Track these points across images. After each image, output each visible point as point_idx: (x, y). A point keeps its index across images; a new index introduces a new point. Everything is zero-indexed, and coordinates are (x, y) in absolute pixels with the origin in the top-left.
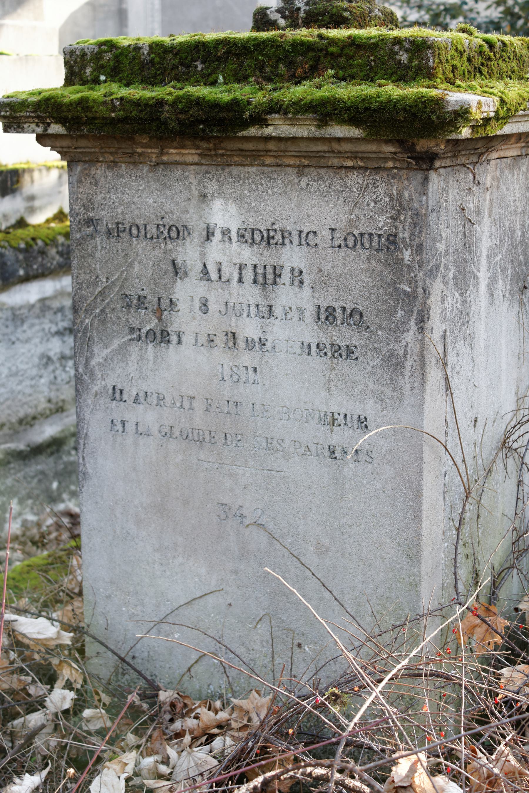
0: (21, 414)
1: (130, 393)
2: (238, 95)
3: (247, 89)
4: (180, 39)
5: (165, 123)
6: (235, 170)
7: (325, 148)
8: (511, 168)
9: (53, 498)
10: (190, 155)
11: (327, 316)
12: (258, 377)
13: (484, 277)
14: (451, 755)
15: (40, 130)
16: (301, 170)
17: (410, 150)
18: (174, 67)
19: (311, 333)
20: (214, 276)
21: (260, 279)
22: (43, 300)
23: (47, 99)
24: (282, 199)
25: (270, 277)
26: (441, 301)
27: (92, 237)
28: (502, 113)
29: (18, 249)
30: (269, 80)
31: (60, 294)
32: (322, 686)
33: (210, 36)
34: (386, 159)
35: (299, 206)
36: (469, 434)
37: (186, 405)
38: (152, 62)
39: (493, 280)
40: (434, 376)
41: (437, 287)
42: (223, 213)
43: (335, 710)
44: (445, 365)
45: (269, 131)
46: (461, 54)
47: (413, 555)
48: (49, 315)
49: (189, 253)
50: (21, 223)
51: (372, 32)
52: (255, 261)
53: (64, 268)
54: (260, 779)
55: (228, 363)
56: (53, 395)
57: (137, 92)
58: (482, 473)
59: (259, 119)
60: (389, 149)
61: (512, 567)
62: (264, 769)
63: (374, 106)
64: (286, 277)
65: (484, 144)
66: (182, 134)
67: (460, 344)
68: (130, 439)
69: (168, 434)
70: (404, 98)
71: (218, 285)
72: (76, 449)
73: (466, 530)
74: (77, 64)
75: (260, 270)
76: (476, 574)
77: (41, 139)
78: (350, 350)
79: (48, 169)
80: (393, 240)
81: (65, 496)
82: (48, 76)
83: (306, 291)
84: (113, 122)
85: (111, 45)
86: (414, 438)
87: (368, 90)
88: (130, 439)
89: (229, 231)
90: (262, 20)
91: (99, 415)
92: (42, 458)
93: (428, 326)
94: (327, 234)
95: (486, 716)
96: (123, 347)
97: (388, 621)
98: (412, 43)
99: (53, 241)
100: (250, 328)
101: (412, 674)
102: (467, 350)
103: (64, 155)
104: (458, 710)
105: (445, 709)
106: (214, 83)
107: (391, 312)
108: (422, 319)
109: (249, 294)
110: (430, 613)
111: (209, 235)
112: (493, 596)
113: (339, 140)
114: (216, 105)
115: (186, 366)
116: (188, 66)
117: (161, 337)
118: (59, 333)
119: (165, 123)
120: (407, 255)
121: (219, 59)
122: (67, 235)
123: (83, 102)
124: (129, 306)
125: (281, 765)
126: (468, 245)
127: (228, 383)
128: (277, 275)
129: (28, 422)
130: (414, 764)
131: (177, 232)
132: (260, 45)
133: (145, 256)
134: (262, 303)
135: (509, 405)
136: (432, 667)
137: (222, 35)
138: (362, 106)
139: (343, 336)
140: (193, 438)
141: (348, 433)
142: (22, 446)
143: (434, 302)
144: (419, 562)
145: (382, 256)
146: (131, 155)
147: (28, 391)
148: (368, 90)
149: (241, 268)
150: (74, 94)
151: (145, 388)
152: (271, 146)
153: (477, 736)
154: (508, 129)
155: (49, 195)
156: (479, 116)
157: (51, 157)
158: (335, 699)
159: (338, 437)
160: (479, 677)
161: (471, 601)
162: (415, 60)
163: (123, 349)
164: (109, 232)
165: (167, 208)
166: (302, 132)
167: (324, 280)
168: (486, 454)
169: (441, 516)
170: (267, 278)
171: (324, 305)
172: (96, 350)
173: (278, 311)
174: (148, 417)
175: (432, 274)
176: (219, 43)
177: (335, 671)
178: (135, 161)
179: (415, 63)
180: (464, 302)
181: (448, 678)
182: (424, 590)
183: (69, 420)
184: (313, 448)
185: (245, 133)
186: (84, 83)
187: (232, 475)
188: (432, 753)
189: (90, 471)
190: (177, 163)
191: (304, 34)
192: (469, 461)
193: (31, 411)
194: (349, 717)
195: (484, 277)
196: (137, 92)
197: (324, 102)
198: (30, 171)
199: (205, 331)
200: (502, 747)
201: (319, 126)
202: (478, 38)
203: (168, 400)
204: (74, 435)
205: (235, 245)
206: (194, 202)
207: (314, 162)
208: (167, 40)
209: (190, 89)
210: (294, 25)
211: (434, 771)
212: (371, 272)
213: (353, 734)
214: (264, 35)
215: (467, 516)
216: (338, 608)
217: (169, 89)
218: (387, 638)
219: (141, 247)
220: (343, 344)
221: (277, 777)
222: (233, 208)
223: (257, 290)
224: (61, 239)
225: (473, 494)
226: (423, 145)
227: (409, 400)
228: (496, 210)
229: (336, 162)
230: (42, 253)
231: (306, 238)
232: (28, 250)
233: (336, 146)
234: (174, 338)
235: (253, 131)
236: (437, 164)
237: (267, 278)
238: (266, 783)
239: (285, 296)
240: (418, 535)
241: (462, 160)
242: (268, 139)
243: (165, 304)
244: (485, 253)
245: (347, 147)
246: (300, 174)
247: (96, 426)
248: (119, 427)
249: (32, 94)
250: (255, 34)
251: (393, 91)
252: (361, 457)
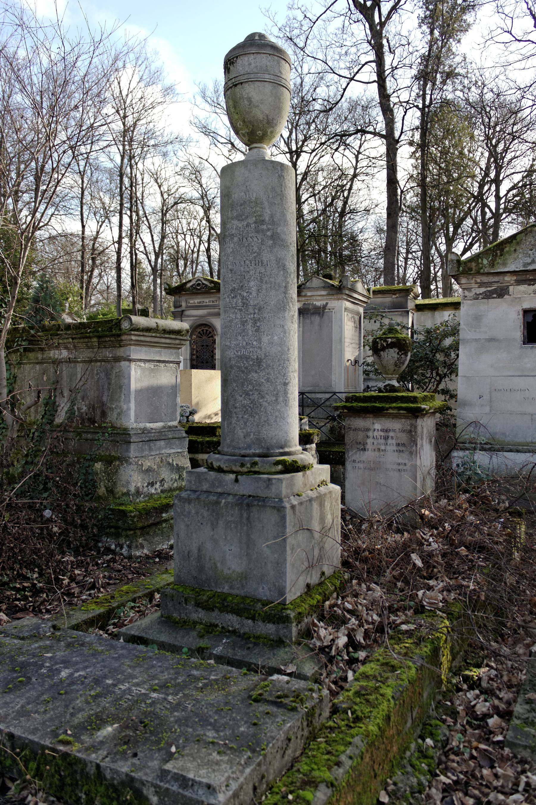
11: (398, 445)
19: (395, 448)
42: (377, 426)
49: (370, 434)
86: (415, 467)
100: (383, 447)
109: (383, 441)
115: (369, 455)
117: (364, 450)
131: (368, 430)
133: (361, 435)
139: (401, 448)
140: (371, 469)
159: (401, 467)
167: (397, 438)
174: (361, 465)
231: (394, 431)
237: (386, 438)
239: (390, 441)
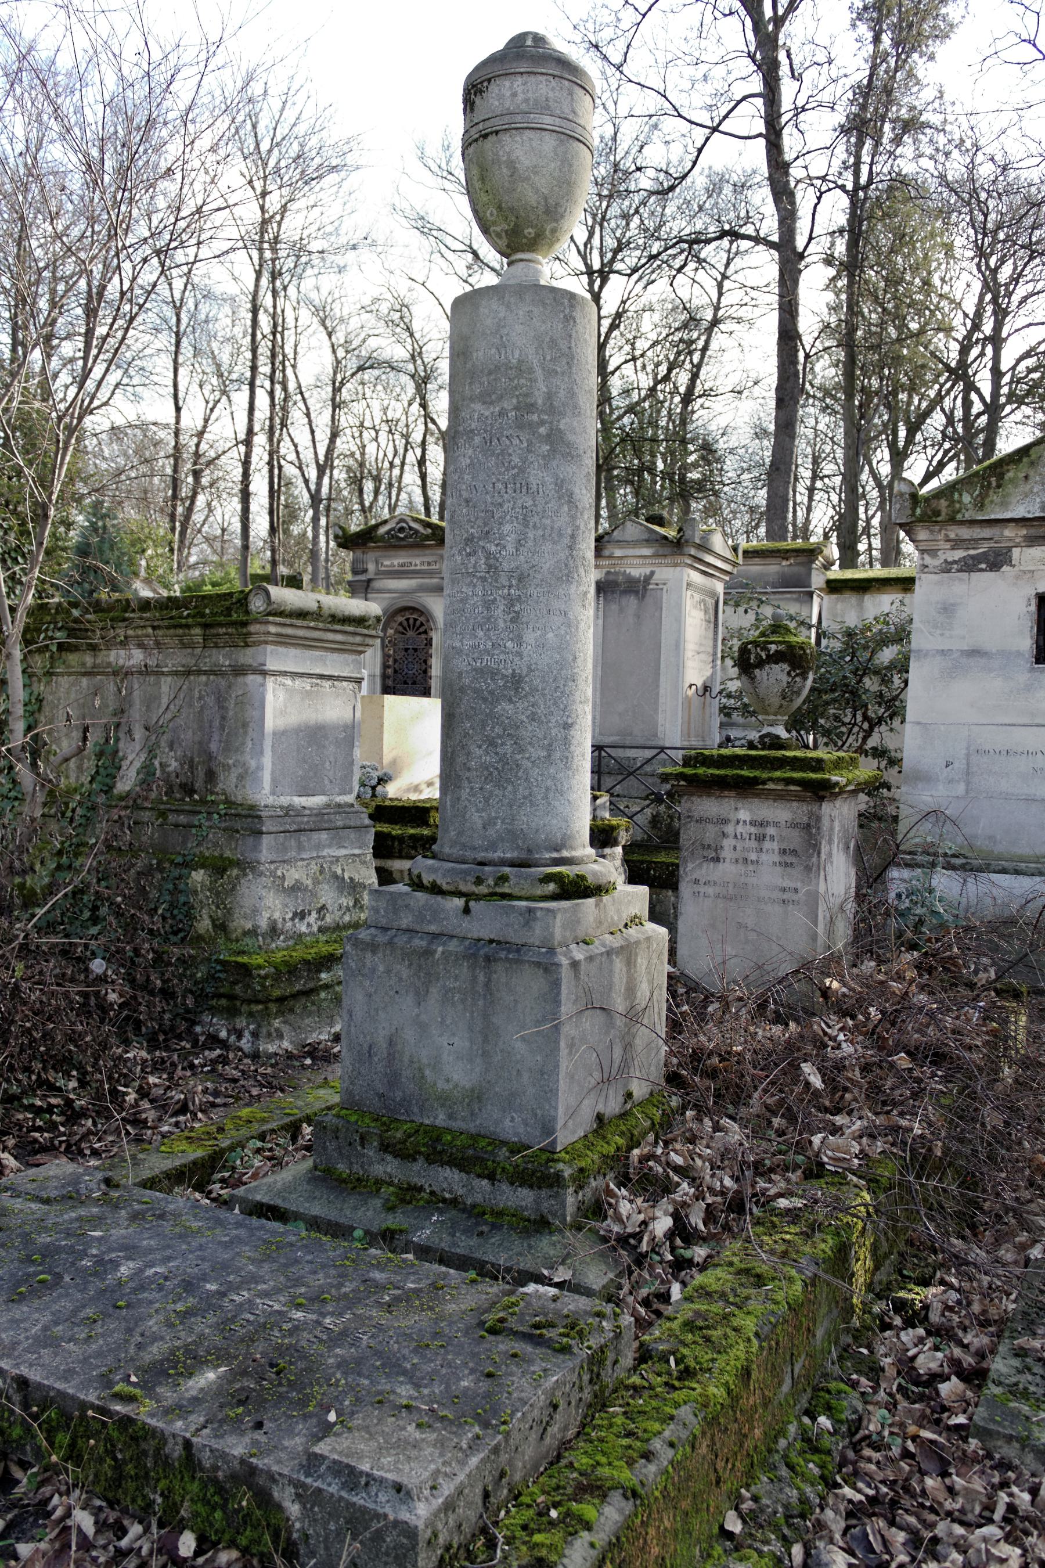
10: (733, 794)
11: (784, 852)
19: (777, 858)
26: (824, 849)
42: (744, 815)
49: (729, 829)
100: (753, 856)
109: (754, 844)
115: (727, 870)
117: (717, 860)
131: (725, 821)
139: (789, 859)
140: (728, 898)
167: (782, 839)
174: (710, 890)
178: (709, 795)
219: (710, 826)
231: (776, 824)
237: (761, 838)
239: (767, 845)
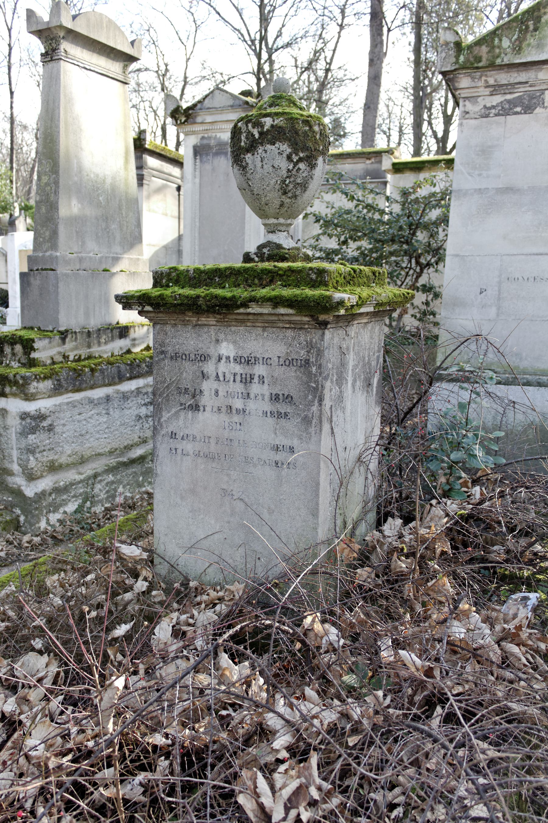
0: (126, 444)
1: (180, 434)
2: (235, 293)
3: (240, 290)
4: (208, 267)
5: (200, 306)
6: (233, 329)
7: (276, 318)
8: (364, 328)
9: (140, 485)
10: (212, 320)
11: (275, 398)
12: (242, 427)
13: (350, 379)
14: (332, 613)
15: (140, 309)
16: (264, 328)
17: (316, 320)
18: (205, 280)
19: (268, 407)
20: (221, 378)
21: (244, 380)
22: (138, 389)
23: (144, 294)
24: (255, 343)
25: (249, 379)
26: (330, 391)
27: (163, 359)
28: (360, 303)
29: (128, 364)
30: (250, 286)
31: (147, 385)
32: (270, 579)
33: (223, 265)
34: (305, 324)
35: (263, 346)
36: (342, 454)
37: (207, 441)
38: (195, 277)
39: (355, 381)
40: (326, 427)
41: (328, 384)
42: (227, 349)
43: (276, 591)
44: (331, 422)
45: (250, 310)
46: (341, 275)
47: (315, 513)
48: (141, 396)
49: (210, 368)
50: (129, 352)
51: (298, 265)
52: (242, 372)
53: (149, 373)
54: (239, 626)
55: (227, 420)
56: (141, 435)
57: (188, 291)
58: (349, 474)
59: (245, 305)
60: (306, 319)
61: (362, 519)
62: (241, 622)
63: (299, 299)
64: (256, 380)
65: (351, 317)
66: (208, 311)
67: (339, 412)
68: (179, 458)
69: (198, 455)
70: (314, 295)
71: (223, 383)
72: (152, 461)
73: (340, 501)
74: (159, 279)
75: (244, 376)
76: (345, 523)
77: (140, 313)
78: (286, 414)
79: (143, 326)
80: (307, 362)
81: (146, 484)
82: (145, 284)
83: (266, 386)
84: (175, 306)
85: (175, 269)
86: (316, 456)
87: (297, 291)
88: (179, 458)
89: (229, 357)
90: (247, 258)
91: (164, 446)
92: (135, 465)
93: (324, 403)
94: (276, 359)
95: (349, 593)
96: (177, 413)
97: (302, 546)
98: (318, 270)
99: (144, 360)
100: (238, 404)
101: (314, 572)
102: (342, 415)
103: (151, 320)
104: (336, 590)
105: (329, 590)
106: (224, 288)
107: (306, 397)
108: (321, 400)
109: (239, 387)
110: (323, 542)
111: (220, 359)
112: (353, 534)
113: (282, 315)
114: (225, 298)
115: (207, 422)
116: (212, 279)
117: (196, 408)
118: (145, 405)
119: (200, 306)
120: (314, 369)
121: (226, 276)
122: (151, 358)
123: (161, 296)
124: (180, 393)
125: (250, 619)
126: (343, 364)
127: (227, 430)
128: (252, 378)
129: (128, 448)
130: (314, 618)
131: (204, 358)
132: (246, 270)
133: (189, 370)
134: (243, 391)
135: (362, 441)
136: (323, 569)
137: (228, 265)
138: (294, 299)
139: (283, 408)
140: (209, 457)
141: (285, 454)
142: (125, 460)
143: (326, 392)
144: (318, 517)
145: (302, 370)
146: (183, 321)
147: (129, 432)
148: (297, 291)
149: (235, 375)
150: (156, 292)
151: (187, 432)
152: (250, 317)
153: (345, 604)
154: (362, 310)
155: (142, 338)
156: (349, 304)
157: (144, 320)
158: (276, 585)
159: (279, 457)
160: (345, 574)
161: (343, 536)
162: (320, 278)
163: (177, 413)
164: (172, 358)
165: (200, 346)
166: (265, 311)
167: (274, 381)
168: (350, 464)
169: (329, 494)
170: (247, 380)
171: (274, 393)
172: (164, 414)
173: (252, 396)
174: (189, 447)
175: (326, 378)
176: (226, 269)
177: (277, 571)
178: (185, 323)
179: (319, 279)
180: (341, 392)
181: (331, 575)
182: (320, 531)
183: (149, 447)
184: (267, 462)
185: (238, 311)
186: (162, 287)
187: (228, 475)
188: (323, 612)
189: (159, 473)
190: (205, 325)
191: (267, 265)
192: (342, 468)
193: (130, 443)
194: (283, 595)
195: (350, 379)
196: (188, 291)
197: (276, 297)
198: (134, 327)
199: (217, 404)
200: (357, 609)
201: (273, 308)
202: (348, 268)
203: (198, 438)
204: (151, 454)
205: (232, 364)
206: (213, 343)
207: (270, 325)
208: (202, 267)
209: (212, 290)
210: (262, 261)
211: (323, 621)
212: (297, 377)
213: (285, 603)
214: (248, 265)
215: (341, 494)
216: (278, 540)
217: (202, 290)
218: (301, 555)
219: (187, 364)
220: (283, 412)
221: (247, 625)
222: (231, 346)
223: (242, 386)
224: (148, 359)
225: (344, 484)
226: (322, 317)
227: (314, 439)
228: (356, 348)
229: (281, 325)
230: (138, 366)
231: (266, 361)
232: (131, 365)
233: (281, 318)
234: (202, 408)
235: (242, 310)
236: (329, 326)
237: (247, 380)
238: (242, 628)
239: (255, 388)
240: (317, 504)
241: (341, 324)
242: (249, 314)
243: (198, 392)
244: (351, 368)
245: (287, 318)
246: (264, 331)
247: (162, 451)
248: (174, 451)
249: (137, 292)
250: (244, 265)
251: (309, 292)
252: (291, 466)
